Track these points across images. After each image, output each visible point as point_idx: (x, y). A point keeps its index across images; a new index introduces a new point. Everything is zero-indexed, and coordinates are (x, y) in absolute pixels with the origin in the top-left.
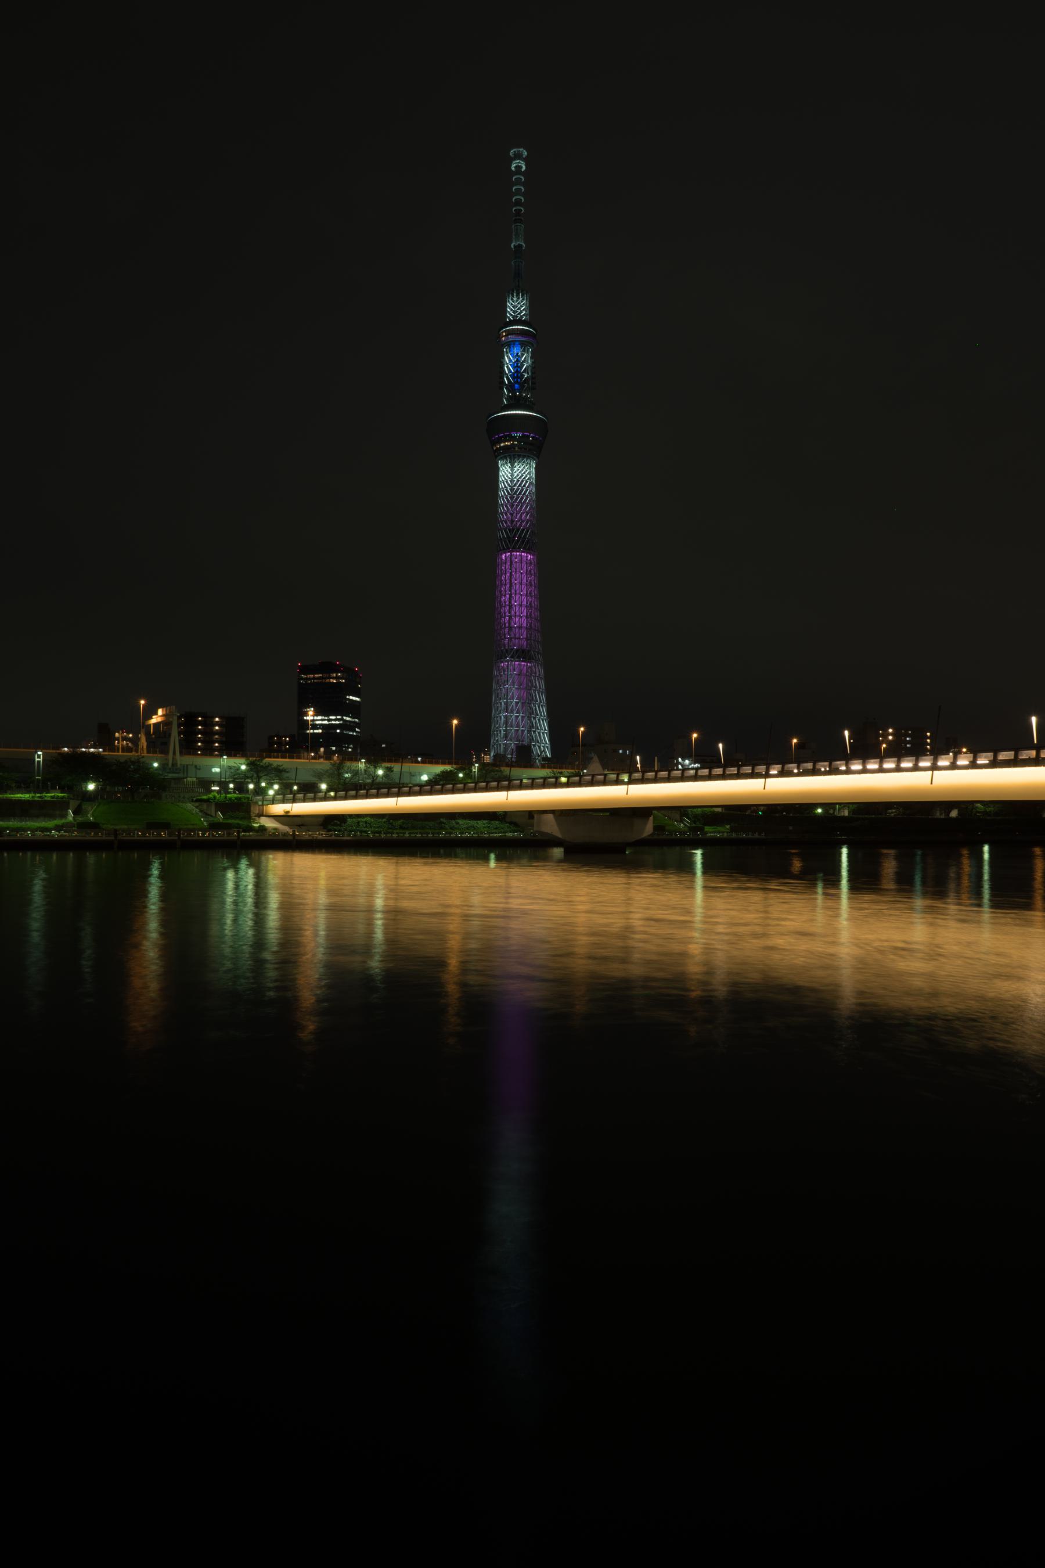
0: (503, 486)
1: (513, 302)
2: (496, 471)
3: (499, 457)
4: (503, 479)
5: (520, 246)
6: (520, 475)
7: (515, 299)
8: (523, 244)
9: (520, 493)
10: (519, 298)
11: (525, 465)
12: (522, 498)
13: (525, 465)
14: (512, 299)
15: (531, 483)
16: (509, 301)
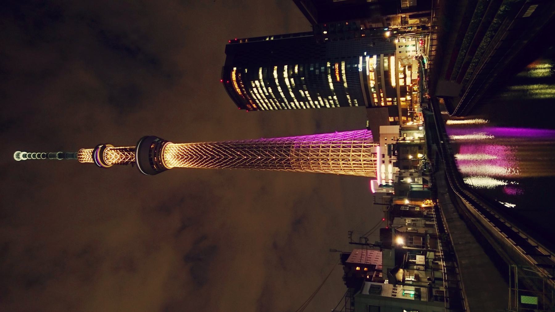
0: (182, 163)
1: (84, 157)
2: (175, 168)
3: (166, 166)
4: (178, 163)
5: (59, 154)
6: (175, 152)
7: (83, 156)
8: (58, 153)
9: (186, 152)
10: (83, 154)
11: (170, 149)
12: (188, 150)
13: (170, 149)
14: (83, 159)
15: (182, 146)
16: (85, 161)
